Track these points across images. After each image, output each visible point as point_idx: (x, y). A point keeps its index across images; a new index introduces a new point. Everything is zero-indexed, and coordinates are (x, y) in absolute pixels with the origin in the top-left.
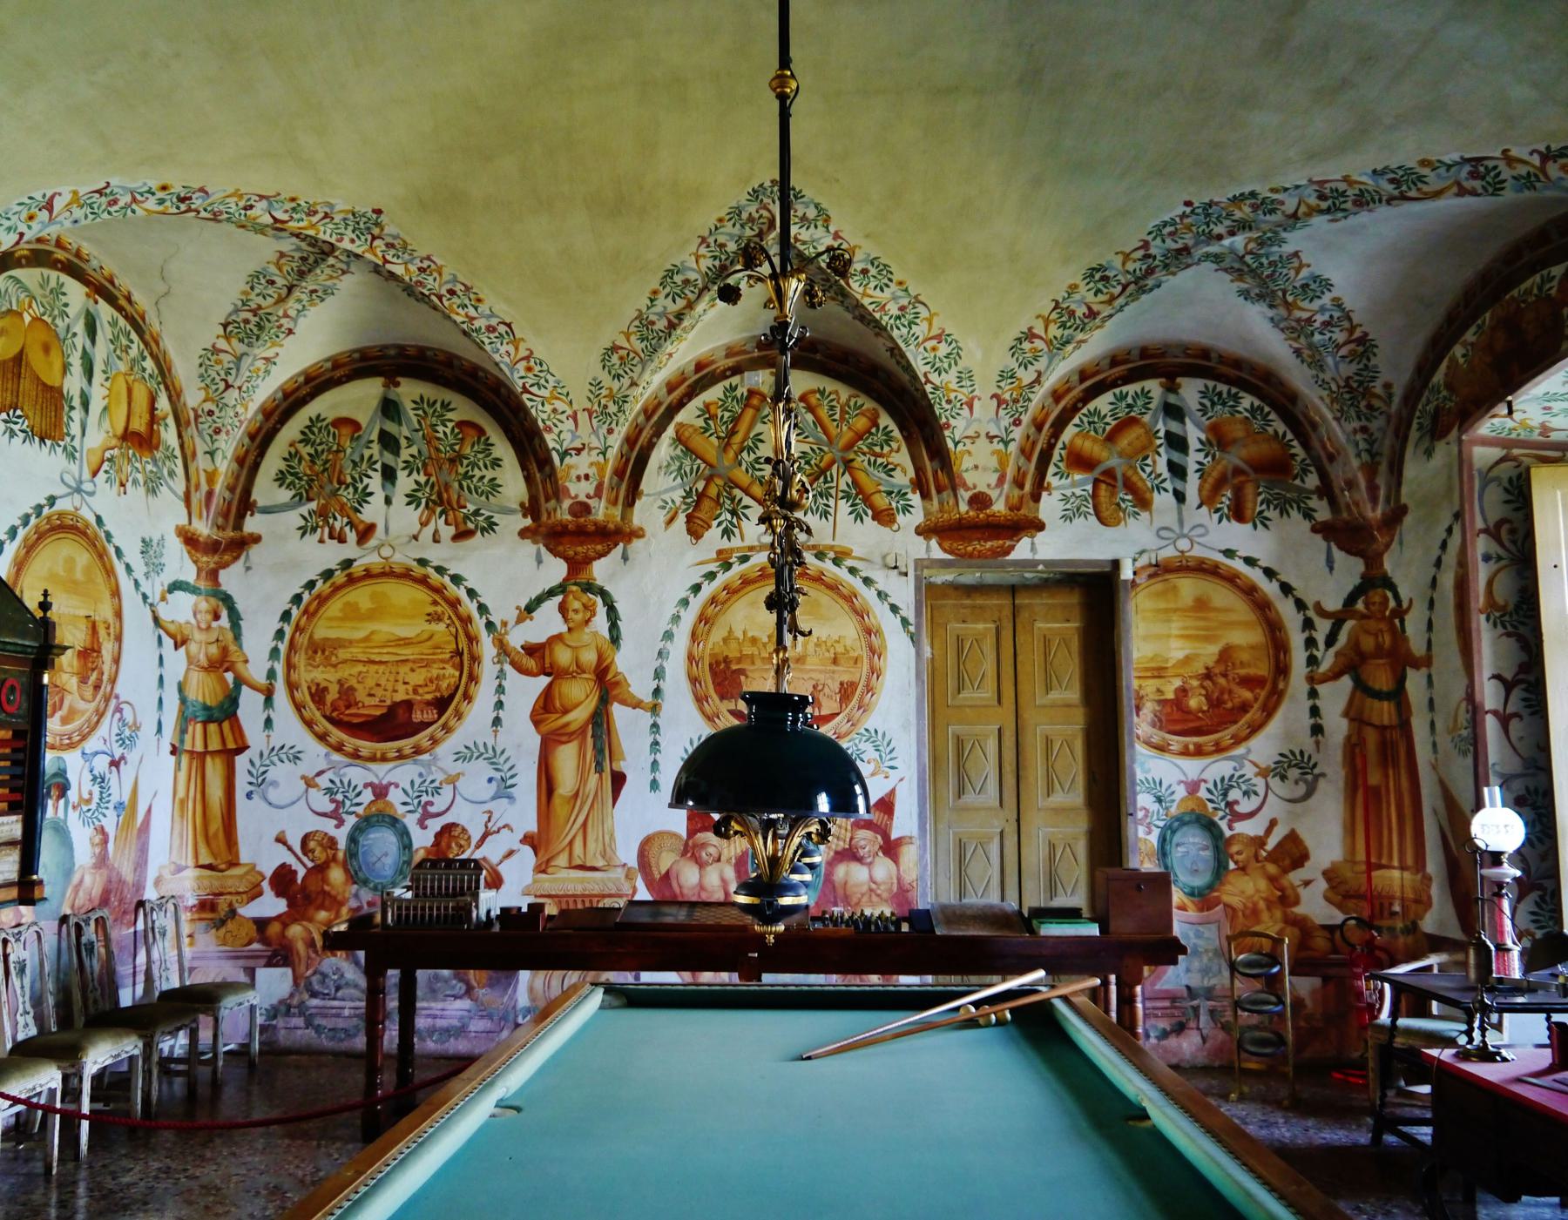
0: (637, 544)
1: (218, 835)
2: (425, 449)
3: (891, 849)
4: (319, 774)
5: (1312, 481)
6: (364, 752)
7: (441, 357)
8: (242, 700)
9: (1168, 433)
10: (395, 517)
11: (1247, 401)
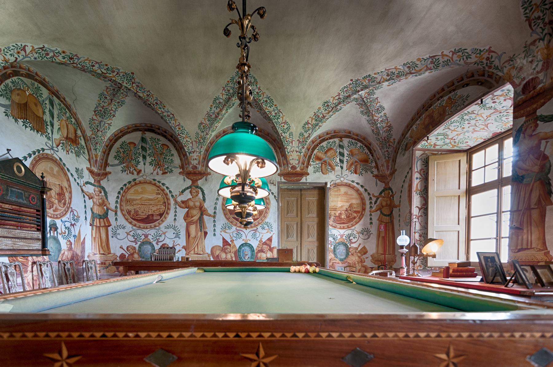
0: (209, 176)
1: (105, 247)
2: (153, 151)
3: (271, 250)
4: (130, 232)
5: (374, 164)
6: (142, 227)
7: (157, 127)
8: (109, 214)
9: (340, 152)
10: (147, 169)
11: (359, 144)
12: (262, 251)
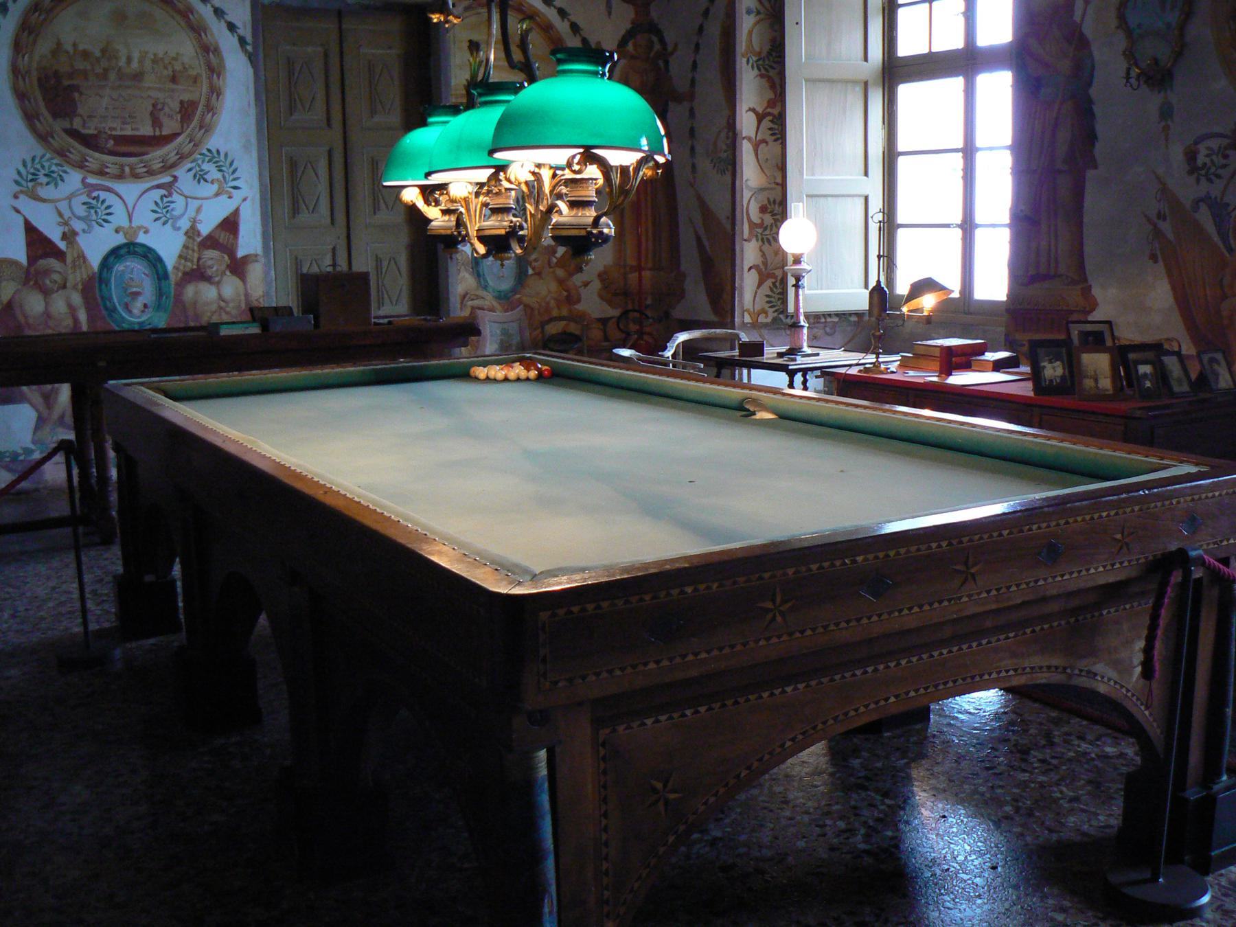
12: (198, 274)
